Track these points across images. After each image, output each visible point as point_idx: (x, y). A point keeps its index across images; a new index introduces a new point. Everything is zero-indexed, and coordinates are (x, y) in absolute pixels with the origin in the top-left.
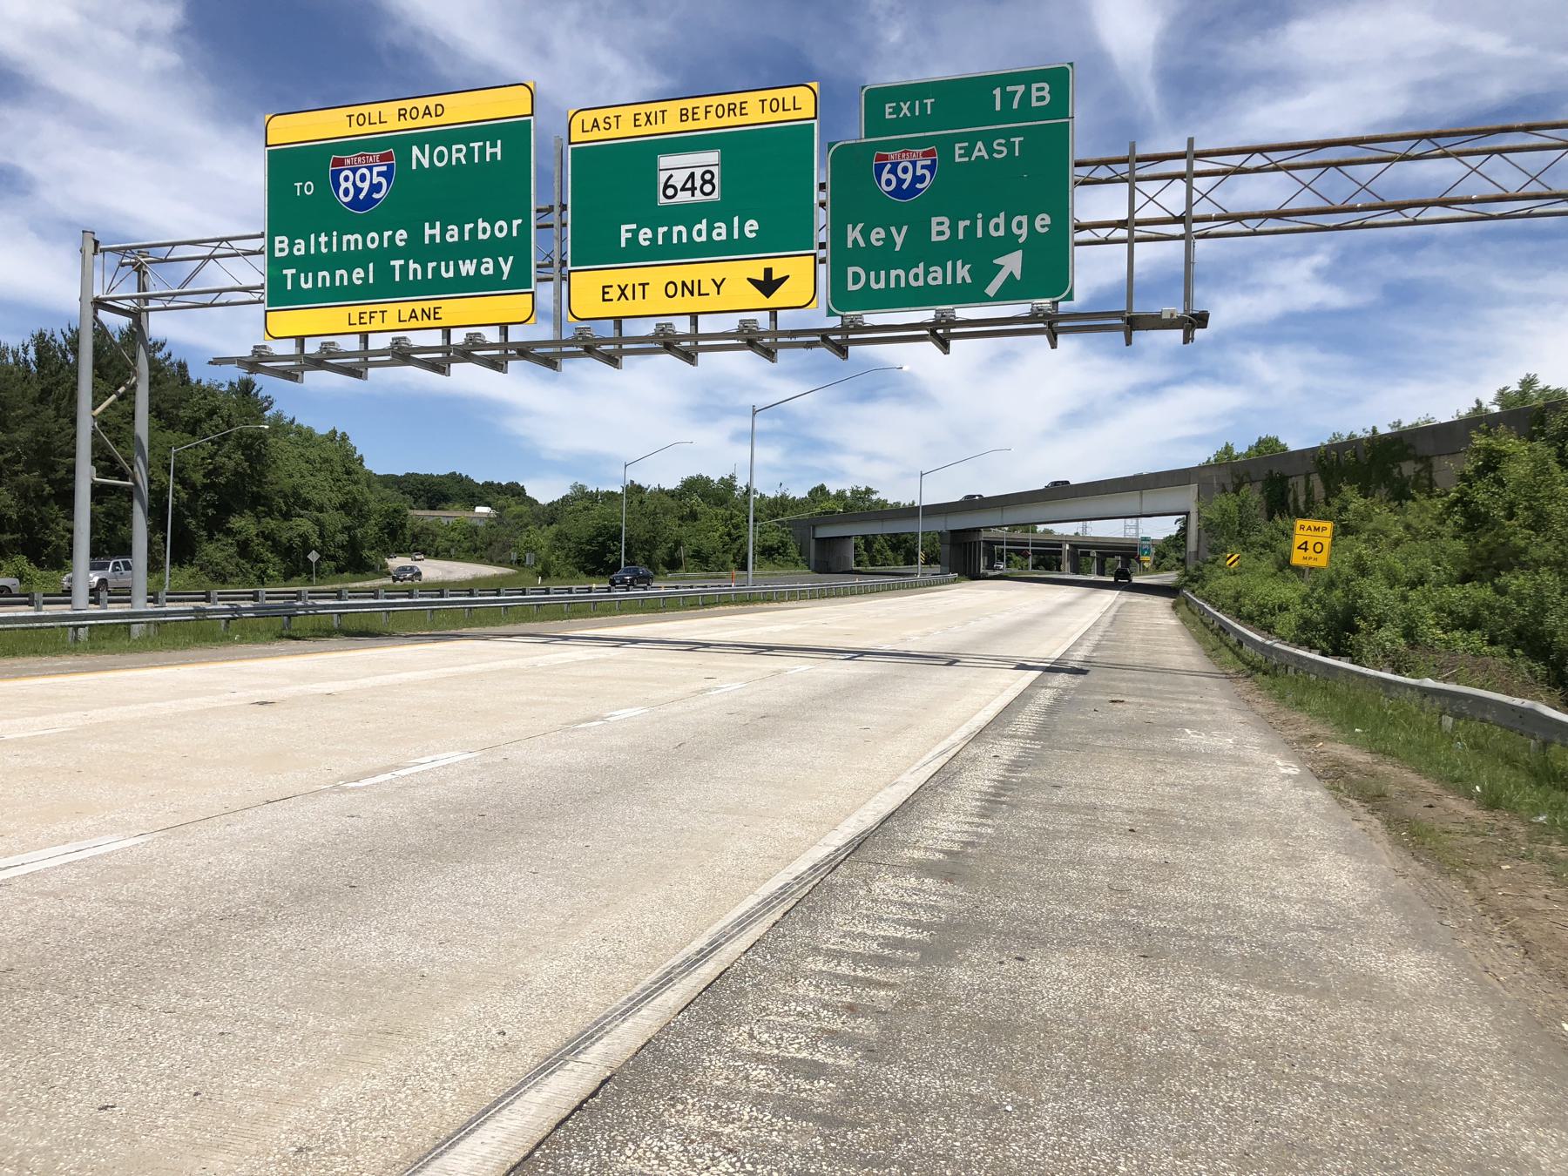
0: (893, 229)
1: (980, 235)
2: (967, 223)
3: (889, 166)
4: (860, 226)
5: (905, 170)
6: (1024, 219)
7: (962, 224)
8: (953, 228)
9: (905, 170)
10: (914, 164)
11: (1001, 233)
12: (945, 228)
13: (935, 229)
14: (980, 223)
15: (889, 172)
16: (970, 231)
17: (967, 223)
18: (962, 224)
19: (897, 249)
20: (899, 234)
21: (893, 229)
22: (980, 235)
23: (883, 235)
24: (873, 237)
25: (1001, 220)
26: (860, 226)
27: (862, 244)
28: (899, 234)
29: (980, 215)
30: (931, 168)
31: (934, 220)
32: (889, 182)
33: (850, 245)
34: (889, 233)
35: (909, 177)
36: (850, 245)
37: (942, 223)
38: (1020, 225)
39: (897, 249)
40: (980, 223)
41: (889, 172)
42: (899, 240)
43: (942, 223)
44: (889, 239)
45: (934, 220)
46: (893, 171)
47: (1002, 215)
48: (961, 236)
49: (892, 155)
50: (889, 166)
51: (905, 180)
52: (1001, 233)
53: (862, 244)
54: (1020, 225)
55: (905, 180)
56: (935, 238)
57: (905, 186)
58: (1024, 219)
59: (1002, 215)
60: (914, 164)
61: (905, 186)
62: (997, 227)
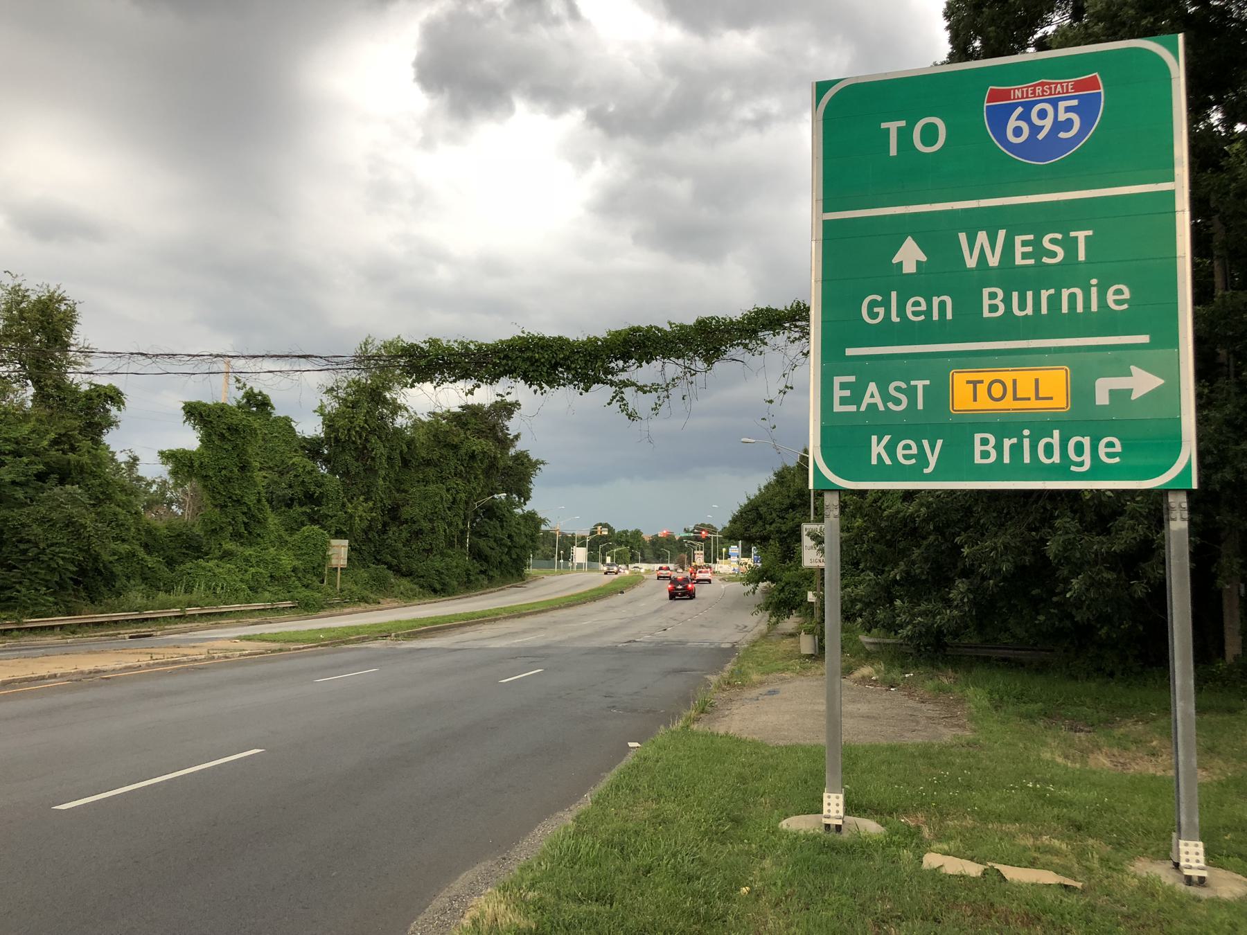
0: (925, 443)
1: (1027, 460)
2: (1014, 440)
7: (1007, 443)
8: (999, 447)
14: (1026, 442)
17: (1014, 440)
18: (1007, 443)
21: (925, 443)
22: (1027, 460)
24: (900, 452)
27: (888, 462)
33: (874, 462)
36: (874, 462)
40: (1026, 442)
42: (933, 460)
48: (1007, 460)
49: (1018, 92)
53: (888, 462)
62: (1049, 450)
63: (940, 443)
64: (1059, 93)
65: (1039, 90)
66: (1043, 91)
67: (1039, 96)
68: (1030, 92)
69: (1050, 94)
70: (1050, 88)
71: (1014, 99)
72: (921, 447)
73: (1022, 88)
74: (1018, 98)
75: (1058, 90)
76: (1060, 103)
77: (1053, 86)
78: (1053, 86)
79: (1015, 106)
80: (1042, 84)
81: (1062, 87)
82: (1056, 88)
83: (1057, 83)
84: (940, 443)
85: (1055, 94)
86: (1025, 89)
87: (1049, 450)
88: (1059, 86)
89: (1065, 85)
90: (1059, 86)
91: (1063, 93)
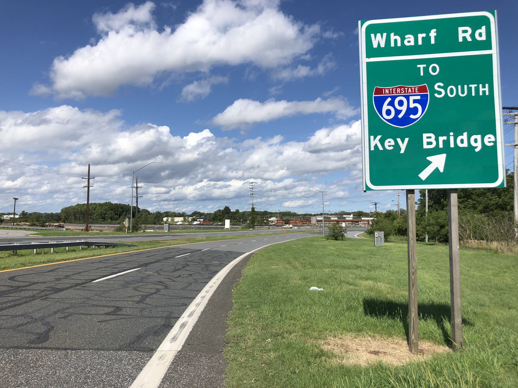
0: (399, 140)
1: (452, 145)
2: (445, 138)
3: (389, 99)
4: (379, 137)
5: (401, 103)
6: (479, 137)
8: (437, 140)
9: (401, 103)
10: (407, 97)
11: (465, 145)
12: (433, 140)
13: (425, 140)
14: (452, 139)
15: (388, 105)
16: (446, 143)
17: (445, 138)
19: (402, 151)
20: (403, 142)
21: (399, 140)
22: (452, 145)
23: (393, 143)
24: (386, 144)
25: (465, 136)
26: (379, 137)
28: (403, 142)
29: (451, 134)
30: (422, 102)
31: (425, 135)
32: (388, 112)
34: (397, 144)
35: (404, 109)
37: (430, 137)
38: (476, 141)
39: (402, 151)
40: (452, 139)
41: (388, 105)
42: (403, 147)
43: (430, 137)
44: (397, 147)
45: (425, 135)
46: (391, 104)
47: (465, 134)
50: (389, 99)
51: (401, 111)
52: (465, 145)
54: (476, 141)
55: (401, 111)
56: (425, 146)
57: (400, 116)
58: (479, 137)
59: (465, 134)
60: (407, 97)
61: (400, 116)
62: (462, 141)
63: (407, 140)
64: (410, 93)
65: (398, 90)
66: (401, 91)
67: (399, 93)
68: (394, 91)
69: (405, 93)
70: (405, 90)
71: (385, 94)
72: (396, 142)
73: (389, 89)
74: (387, 94)
75: (409, 91)
76: (410, 97)
77: (406, 89)
78: (406, 89)
79: (387, 98)
80: (400, 87)
81: (412, 90)
82: (408, 90)
83: (408, 88)
84: (407, 140)
85: (408, 93)
86: (391, 89)
87: (462, 141)
88: (410, 89)
89: (413, 88)
90: (410, 89)
91: (412, 93)
